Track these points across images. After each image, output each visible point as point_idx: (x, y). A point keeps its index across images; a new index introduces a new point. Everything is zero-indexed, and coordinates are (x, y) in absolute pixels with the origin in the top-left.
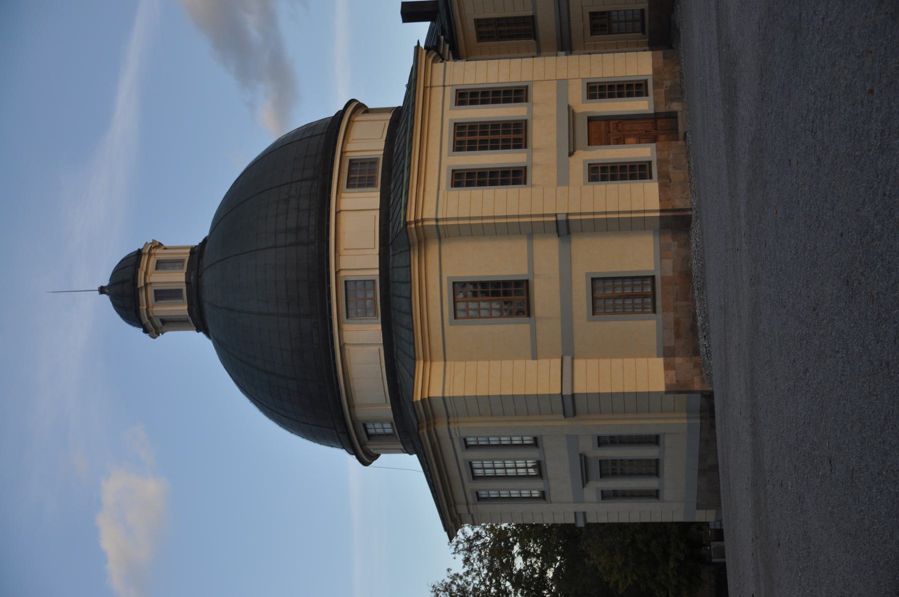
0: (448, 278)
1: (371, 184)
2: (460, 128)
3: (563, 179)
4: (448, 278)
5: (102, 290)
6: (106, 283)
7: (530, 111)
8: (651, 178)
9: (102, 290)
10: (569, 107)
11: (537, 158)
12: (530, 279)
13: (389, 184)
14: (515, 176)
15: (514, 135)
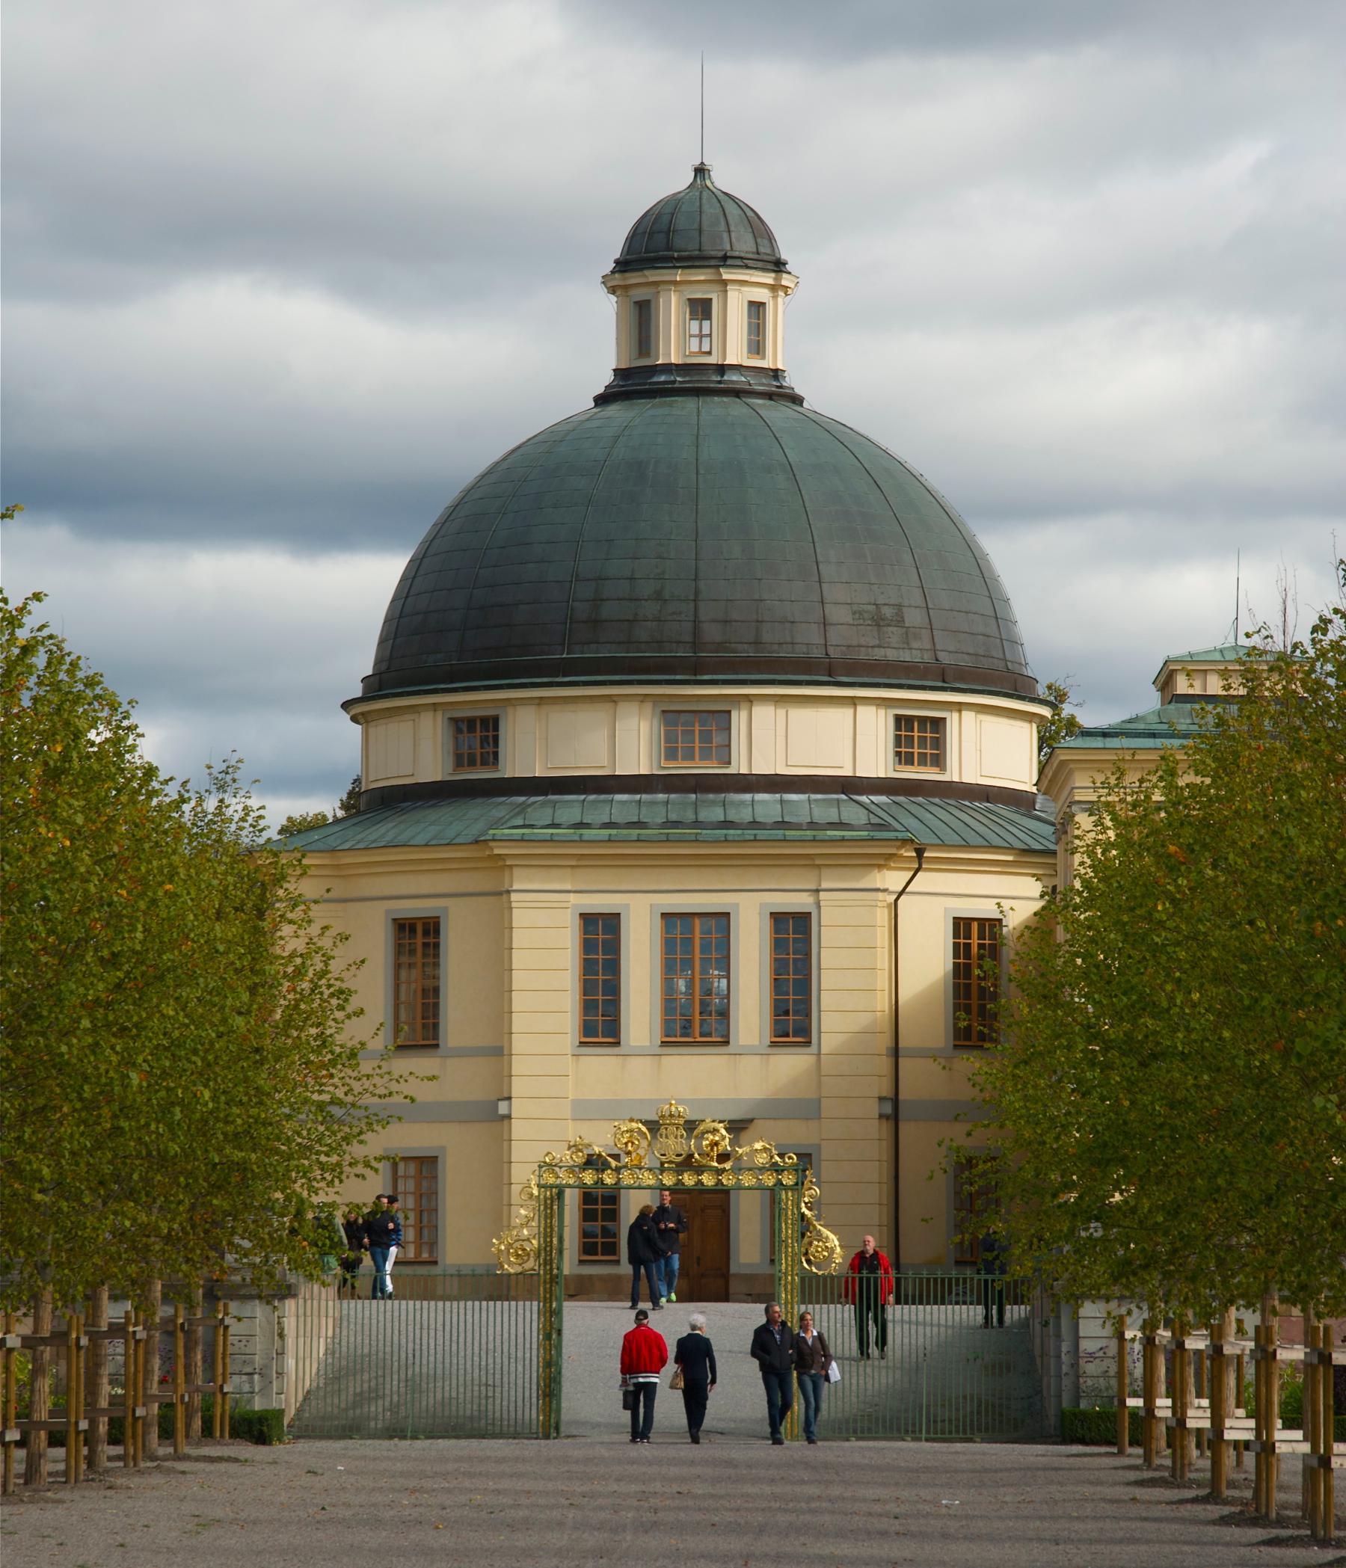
0: (446, 909)
1: (671, 754)
2: (723, 918)
3: (584, 1111)
4: (446, 909)
5: (701, 171)
6: (722, 179)
7: (751, 1052)
8: (581, 1262)
9: (701, 171)
10: (751, 1121)
11: (640, 1066)
12: (440, 1051)
13: (668, 790)
14: (601, 1022)
15: (696, 1021)
